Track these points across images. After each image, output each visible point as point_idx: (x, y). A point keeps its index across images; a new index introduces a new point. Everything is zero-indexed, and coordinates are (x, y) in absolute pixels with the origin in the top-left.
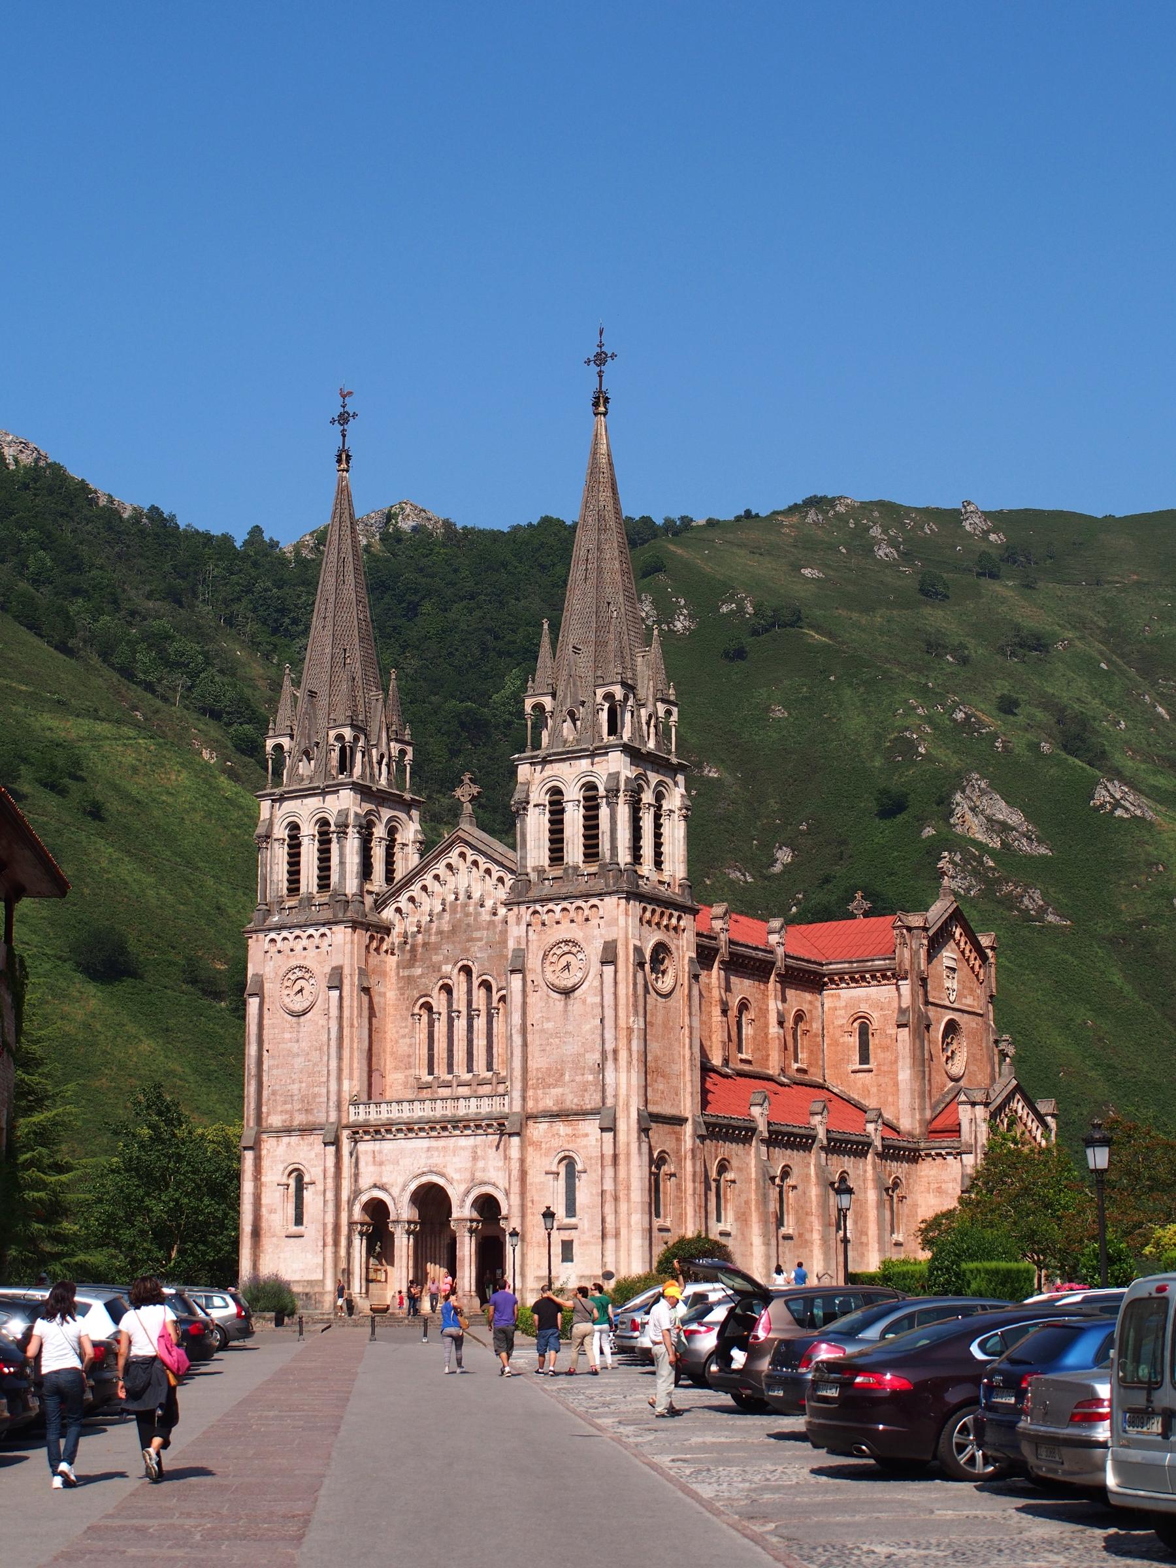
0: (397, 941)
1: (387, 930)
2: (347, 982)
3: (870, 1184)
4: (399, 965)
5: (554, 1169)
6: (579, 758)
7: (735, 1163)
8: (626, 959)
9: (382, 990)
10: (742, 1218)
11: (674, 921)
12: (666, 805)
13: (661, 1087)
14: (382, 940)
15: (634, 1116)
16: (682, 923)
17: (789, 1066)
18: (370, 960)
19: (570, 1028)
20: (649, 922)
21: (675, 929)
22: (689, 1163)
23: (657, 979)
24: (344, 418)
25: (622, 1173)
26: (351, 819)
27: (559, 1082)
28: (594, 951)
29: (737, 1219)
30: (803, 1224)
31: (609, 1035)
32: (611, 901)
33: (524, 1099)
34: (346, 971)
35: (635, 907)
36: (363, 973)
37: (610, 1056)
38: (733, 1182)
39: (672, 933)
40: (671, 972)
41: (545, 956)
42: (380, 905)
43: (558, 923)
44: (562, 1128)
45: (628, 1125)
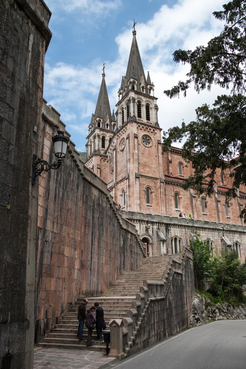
0: (109, 159)
1: (107, 157)
2: (95, 167)
3: (237, 205)
4: (110, 164)
5: (121, 194)
6: (125, 98)
7: (181, 193)
8: (132, 138)
9: (106, 169)
10: (186, 208)
11: (152, 131)
12: (151, 106)
13: (148, 170)
14: (106, 159)
15: (135, 175)
16: (156, 132)
17: (220, 184)
18: (102, 163)
19: (123, 158)
20: (141, 129)
21: (152, 132)
22: (159, 190)
23: (147, 144)
24: (104, 68)
25: (131, 189)
26: (97, 135)
27: (122, 172)
28: (125, 138)
29: (183, 208)
30: (211, 212)
31: (128, 156)
32: (129, 125)
33: (116, 179)
34: (94, 165)
35: (135, 125)
36: (98, 165)
37: (128, 161)
38: (181, 198)
39: (151, 134)
40: (151, 143)
41: (120, 144)
42: (106, 153)
43: (121, 135)
44: (122, 183)
45: (132, 178)
